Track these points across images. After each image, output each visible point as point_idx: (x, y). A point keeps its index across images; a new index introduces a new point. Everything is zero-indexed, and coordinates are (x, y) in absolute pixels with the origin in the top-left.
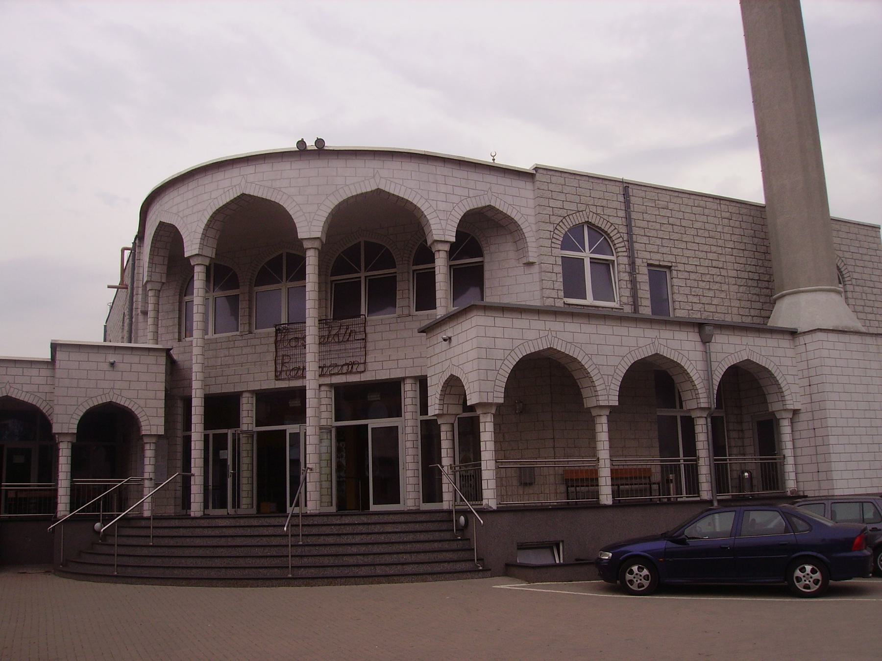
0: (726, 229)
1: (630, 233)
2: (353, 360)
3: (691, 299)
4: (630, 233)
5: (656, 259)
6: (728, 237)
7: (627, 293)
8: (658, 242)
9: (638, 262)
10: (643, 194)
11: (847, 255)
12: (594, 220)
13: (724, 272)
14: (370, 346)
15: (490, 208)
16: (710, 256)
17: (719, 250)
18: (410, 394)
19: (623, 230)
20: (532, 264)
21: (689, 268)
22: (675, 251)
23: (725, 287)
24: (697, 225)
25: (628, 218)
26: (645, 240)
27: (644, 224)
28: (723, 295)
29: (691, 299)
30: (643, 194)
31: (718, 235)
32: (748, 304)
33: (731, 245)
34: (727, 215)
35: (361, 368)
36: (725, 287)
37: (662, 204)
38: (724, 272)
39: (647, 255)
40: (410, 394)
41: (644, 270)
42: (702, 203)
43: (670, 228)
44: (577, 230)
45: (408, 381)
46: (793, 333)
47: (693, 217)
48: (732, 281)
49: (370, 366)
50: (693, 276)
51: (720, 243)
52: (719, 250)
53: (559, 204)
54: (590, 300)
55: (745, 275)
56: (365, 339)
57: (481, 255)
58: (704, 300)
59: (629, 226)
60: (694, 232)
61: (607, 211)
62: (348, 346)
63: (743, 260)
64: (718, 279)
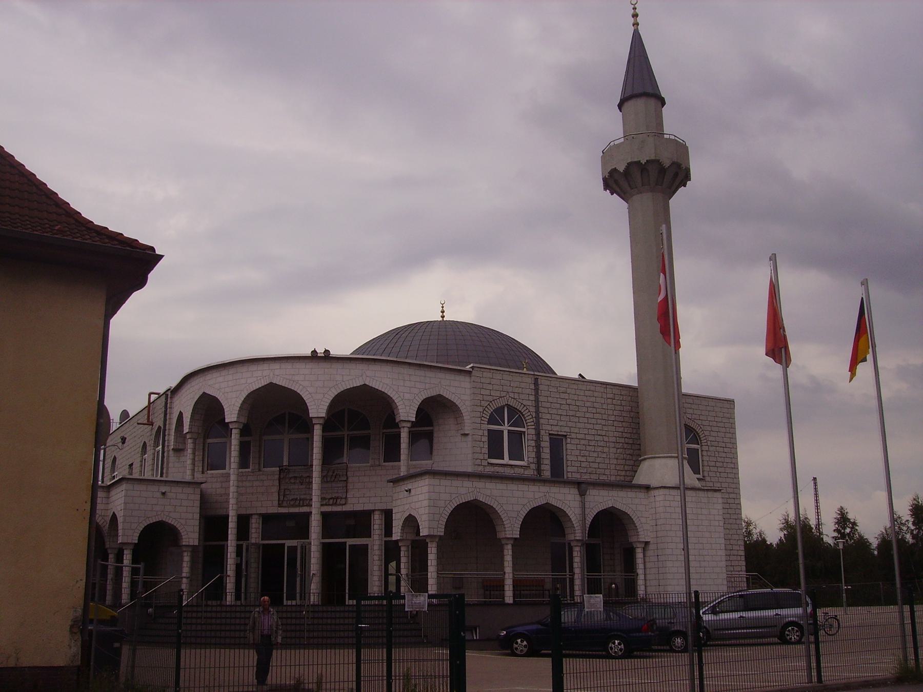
0: (610, 407)
1: (537, 412)
2: (336, 495)
3: (580, 458)
4: (537, 412)
5: (555, 430)
6: (610, 412)
7: (533, 455)
8: (558, 418)
9: (542, 432)
10: (548, 383)
11: (704, 423)
12: (512, 403)
13: (606, 439)
14: (350, 486)
15: (440, 396)
16: (597, 427)
17: (603, 422)
18: (378, 522)
19: (533, 409)
20: (467, 435)
21: (580, 436)
22: (570, 424)
23: (606, 450)
24: (588, 404)
25: (537, 401)
26: (548, 416)
27: (548, 405)
28: (605, 455)
29: (580, 458)
30: (548, 383)
31: (603, 412)
32: (623, 462)
33: (613, 418)
34: (611, 396)
35: (343, 501)
36: (606, 450)
37: (562, 390)
38: (606, 439)
39: (549, 428)
40: (378, 522)
41: (547, 438)
42: (593, 388)
43: (567, 407)
44: (499, 411)
45: (377, 513)
46: (647, 488)
47: (585, 399)
48: (612, 445)
49: (350, 501)
50: (583, 442)
51: (605, 417)
52: (603, 422)
53: (488, 392)
54: (506, 460)
55: (622, 440)
56: (346, 481)
57: (432, 426)
58: (590, 459)
59: (537, 407)
60: (585, 409)
61: (522, 397)
62: (334, 485)
63: (621, 429)
64: (602, 444)
